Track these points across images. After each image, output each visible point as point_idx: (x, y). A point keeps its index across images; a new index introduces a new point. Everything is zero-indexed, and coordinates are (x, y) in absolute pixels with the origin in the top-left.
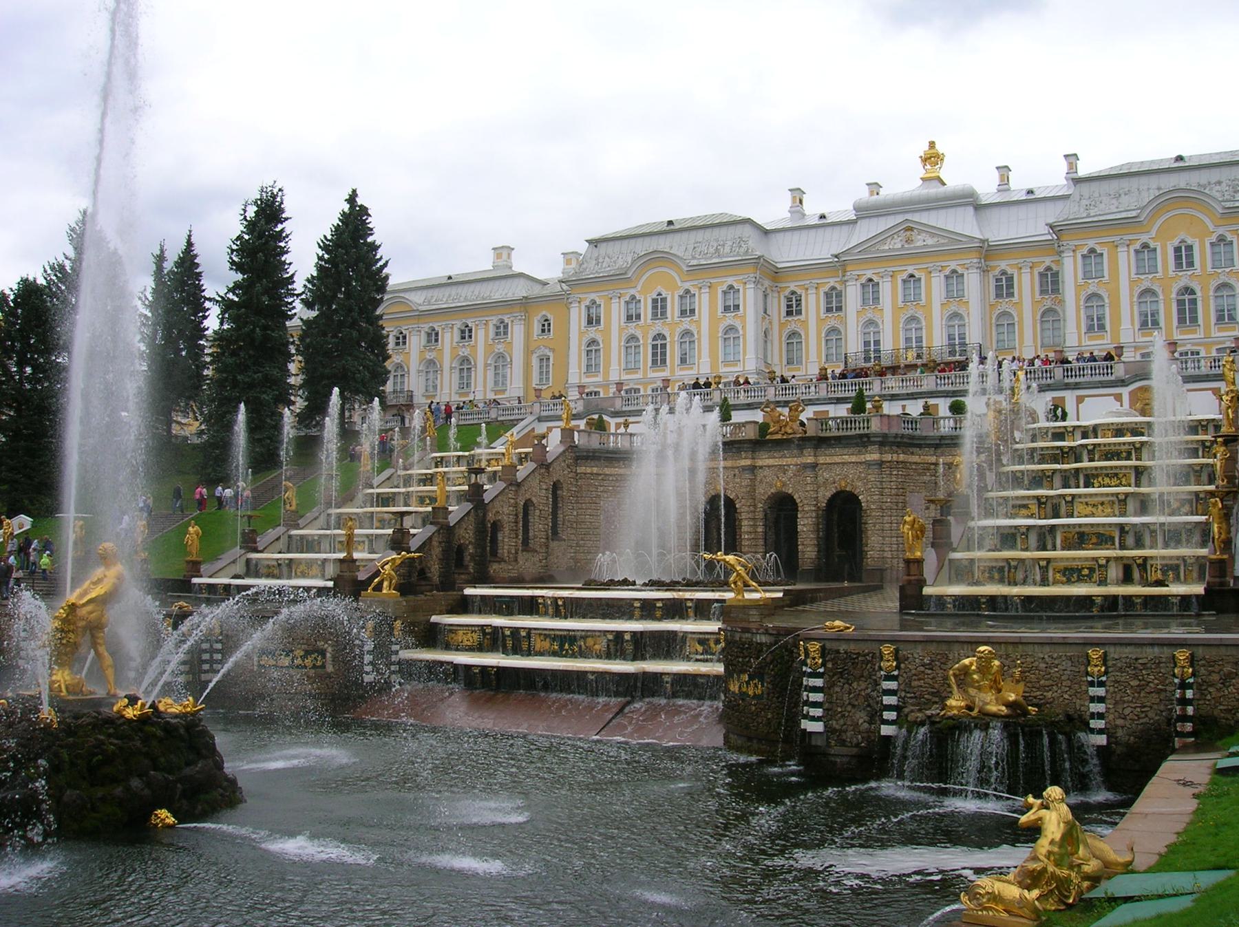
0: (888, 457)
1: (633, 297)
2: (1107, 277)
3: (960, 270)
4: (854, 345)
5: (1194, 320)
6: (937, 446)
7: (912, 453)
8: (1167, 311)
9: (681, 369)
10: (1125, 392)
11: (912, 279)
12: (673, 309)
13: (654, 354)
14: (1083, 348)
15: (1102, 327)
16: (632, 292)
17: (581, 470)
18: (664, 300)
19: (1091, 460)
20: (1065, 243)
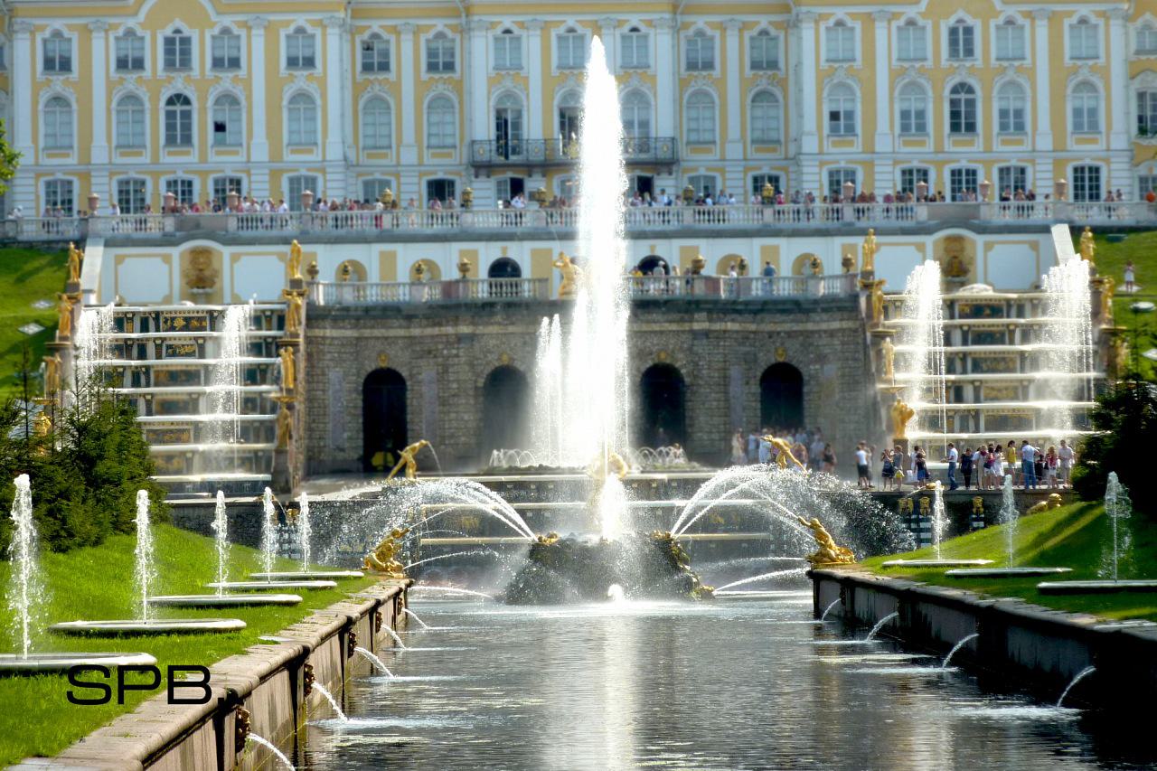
0: (717, 326)
1: (130, 33)
2: (858, 64)
3: (644, 29)
4: (484, 129)
5: (971, 127)
6: (756, 313)
7: (733, 321)
8: (938, 115)
9: (218, 153)
10: (929, 241)
11: (571, 35)
12: (201, 54)
13: (170, 127)
14: (824, 157)
15: (850, 129)
16: (131, 23)
17: (318, 332)
18: (186, 41)
19: (965, 343)
20: (804, 9)
